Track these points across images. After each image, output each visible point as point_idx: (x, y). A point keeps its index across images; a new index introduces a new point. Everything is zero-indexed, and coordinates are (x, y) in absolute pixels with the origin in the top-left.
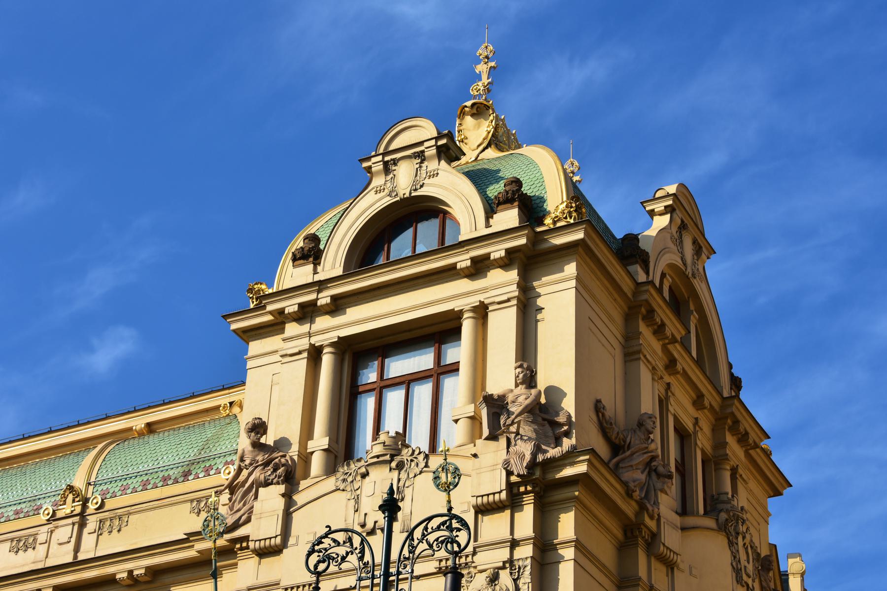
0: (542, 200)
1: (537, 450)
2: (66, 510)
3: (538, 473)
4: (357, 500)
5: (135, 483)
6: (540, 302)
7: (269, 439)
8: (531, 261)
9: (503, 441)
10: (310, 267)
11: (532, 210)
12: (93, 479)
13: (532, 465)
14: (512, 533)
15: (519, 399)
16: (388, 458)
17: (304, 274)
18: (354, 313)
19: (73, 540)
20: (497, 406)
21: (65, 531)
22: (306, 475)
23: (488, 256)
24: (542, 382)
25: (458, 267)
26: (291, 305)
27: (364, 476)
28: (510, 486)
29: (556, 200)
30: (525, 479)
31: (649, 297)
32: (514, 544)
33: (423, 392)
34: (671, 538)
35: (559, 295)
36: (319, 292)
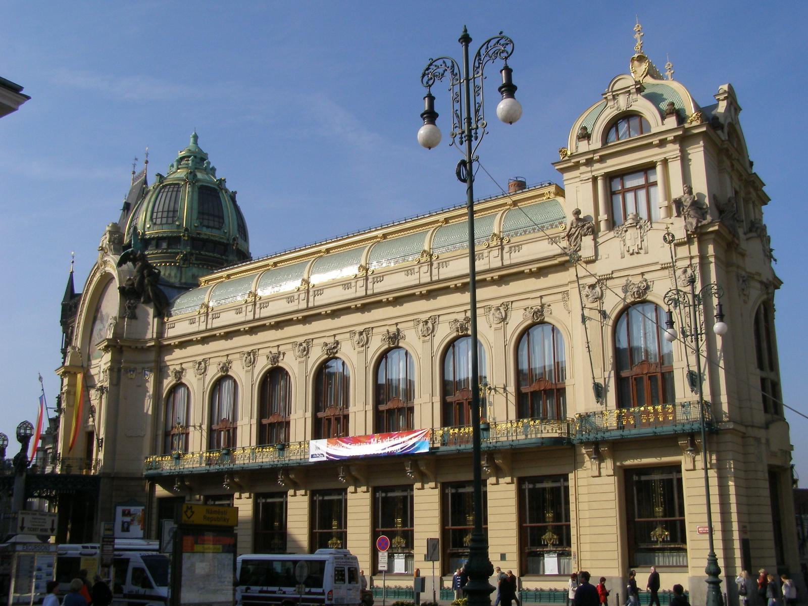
0: (684, 110)
1: (698, 222)
2: (494, 243)
3: (699, 230)
4: (624, 241)
5: (521, 231)
6: (690, 157)
7: (581, 216)
8: (684, 139)
9: (683, 217)
10: (586, 141)
11: (681, 117)
12: (501, 230)
13: (697, 227)
14: (690, 254)
15: (687, 202)
16: (635, 224)
17: (584, 146)
18: (610, 162)
19: (500, 255)
20: (679, 203)
21: (495, 252)
22: (599, 230)
23: (666, 139)
24: (694, 192)
25: (654, 143)
26: (582, 160)
27: (626, 231)
28: (688, 235)
29: (691, 111)
30: (693, 233)
31: (722, 137)
32: (691, 258)
33: (642, 194)
34: (743, 245)
35: (697, 155)
36: (594, 154)
